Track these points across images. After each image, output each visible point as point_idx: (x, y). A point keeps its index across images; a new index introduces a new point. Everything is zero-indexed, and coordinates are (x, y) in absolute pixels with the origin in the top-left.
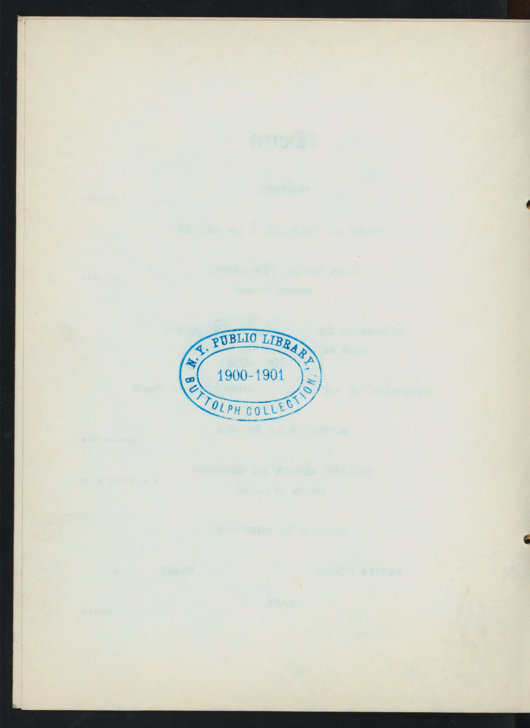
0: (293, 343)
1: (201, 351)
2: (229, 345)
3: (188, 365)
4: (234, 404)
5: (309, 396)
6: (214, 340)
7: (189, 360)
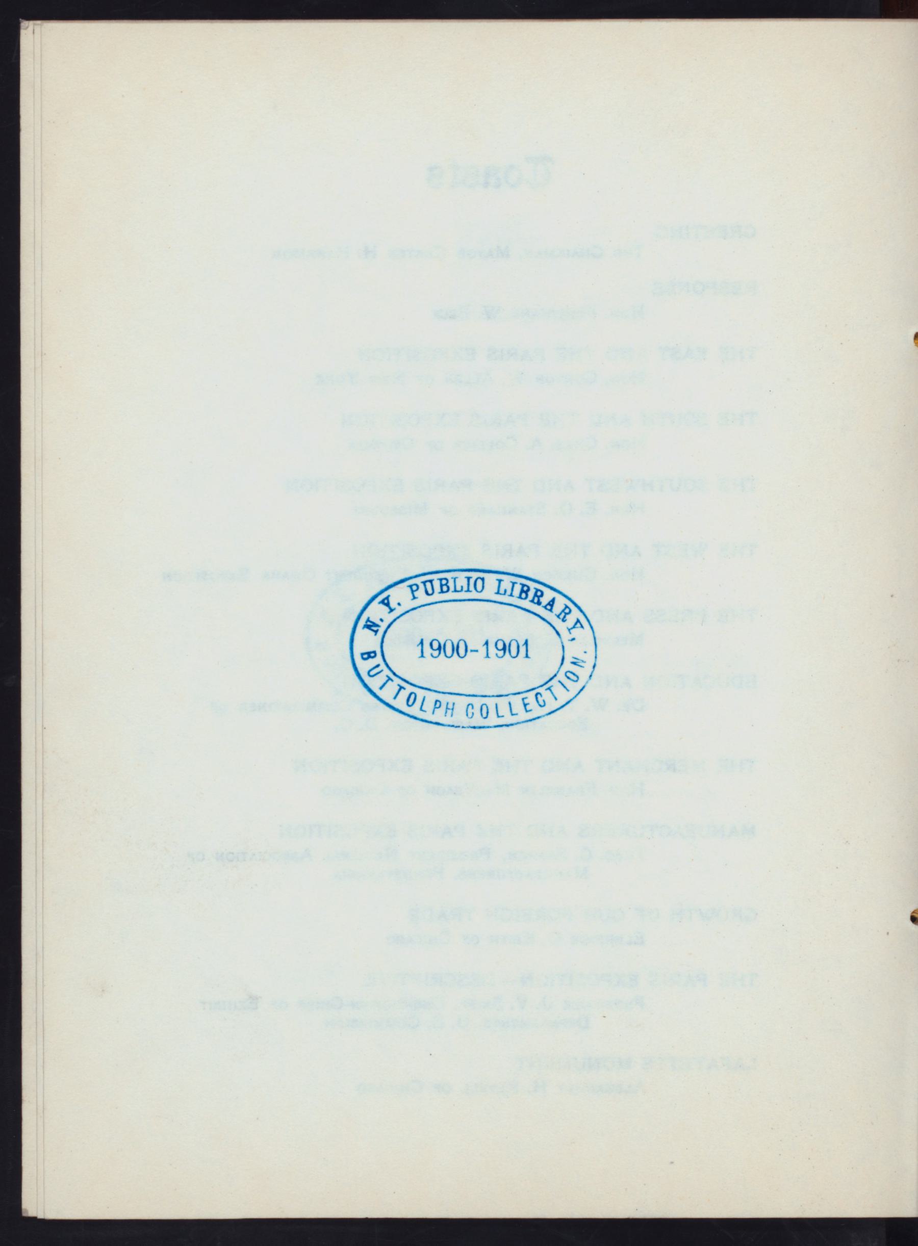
0: (548, 595)
1: (388, 605)
2: (437, 597)
6: (411, 586)
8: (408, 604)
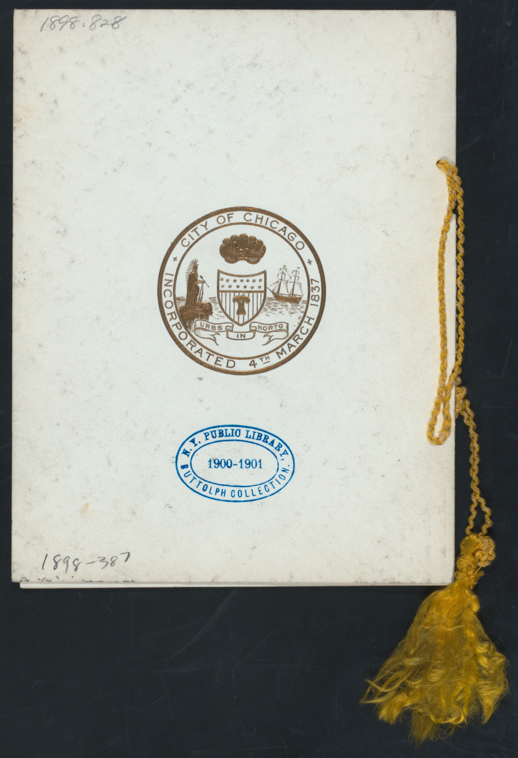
0: (271, 438)
2: (218, 439)
3: (183, 454)
4: (221, 488)
5: (283, 483)
6: (205, 434)
7: (184, 450)
8: (204, 442)
